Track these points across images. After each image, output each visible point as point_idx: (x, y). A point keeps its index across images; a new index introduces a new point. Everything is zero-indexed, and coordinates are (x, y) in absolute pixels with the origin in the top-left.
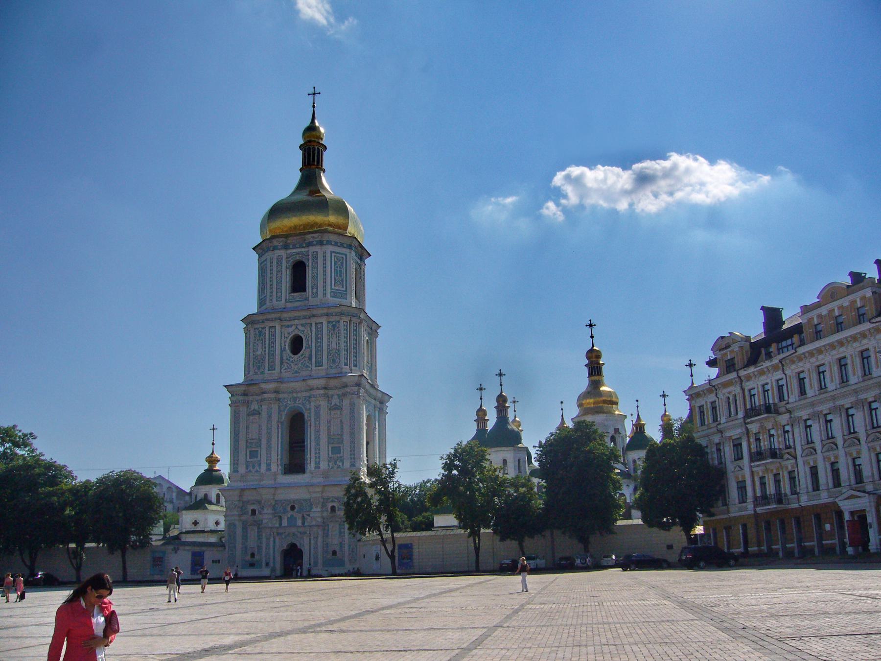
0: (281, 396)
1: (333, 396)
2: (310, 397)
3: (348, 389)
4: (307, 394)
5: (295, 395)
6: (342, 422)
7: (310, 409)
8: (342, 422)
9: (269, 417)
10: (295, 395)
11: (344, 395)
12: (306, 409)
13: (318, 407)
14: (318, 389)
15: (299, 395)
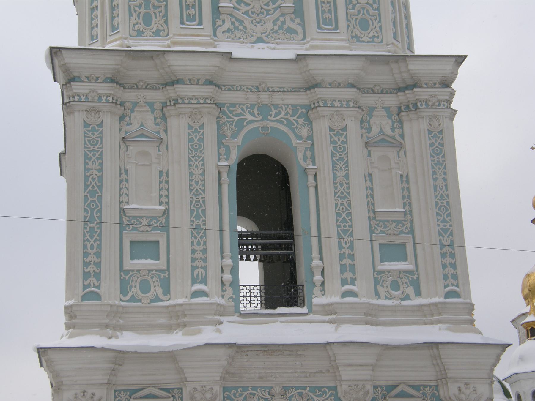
0: (226, 97)
1: (372, 110)
2: (309, 108)
3: (422, 93)
4: (302, 99)
5: (265, 97)
6: (405, 179)
7: (311, 137)
8: (405, 179)
9: (196, 148)
10: (265, 97)
11: (414, 107)
12: (299, 137)
13: (338, 133)
14: (339, 86)
15: (277, 99)
